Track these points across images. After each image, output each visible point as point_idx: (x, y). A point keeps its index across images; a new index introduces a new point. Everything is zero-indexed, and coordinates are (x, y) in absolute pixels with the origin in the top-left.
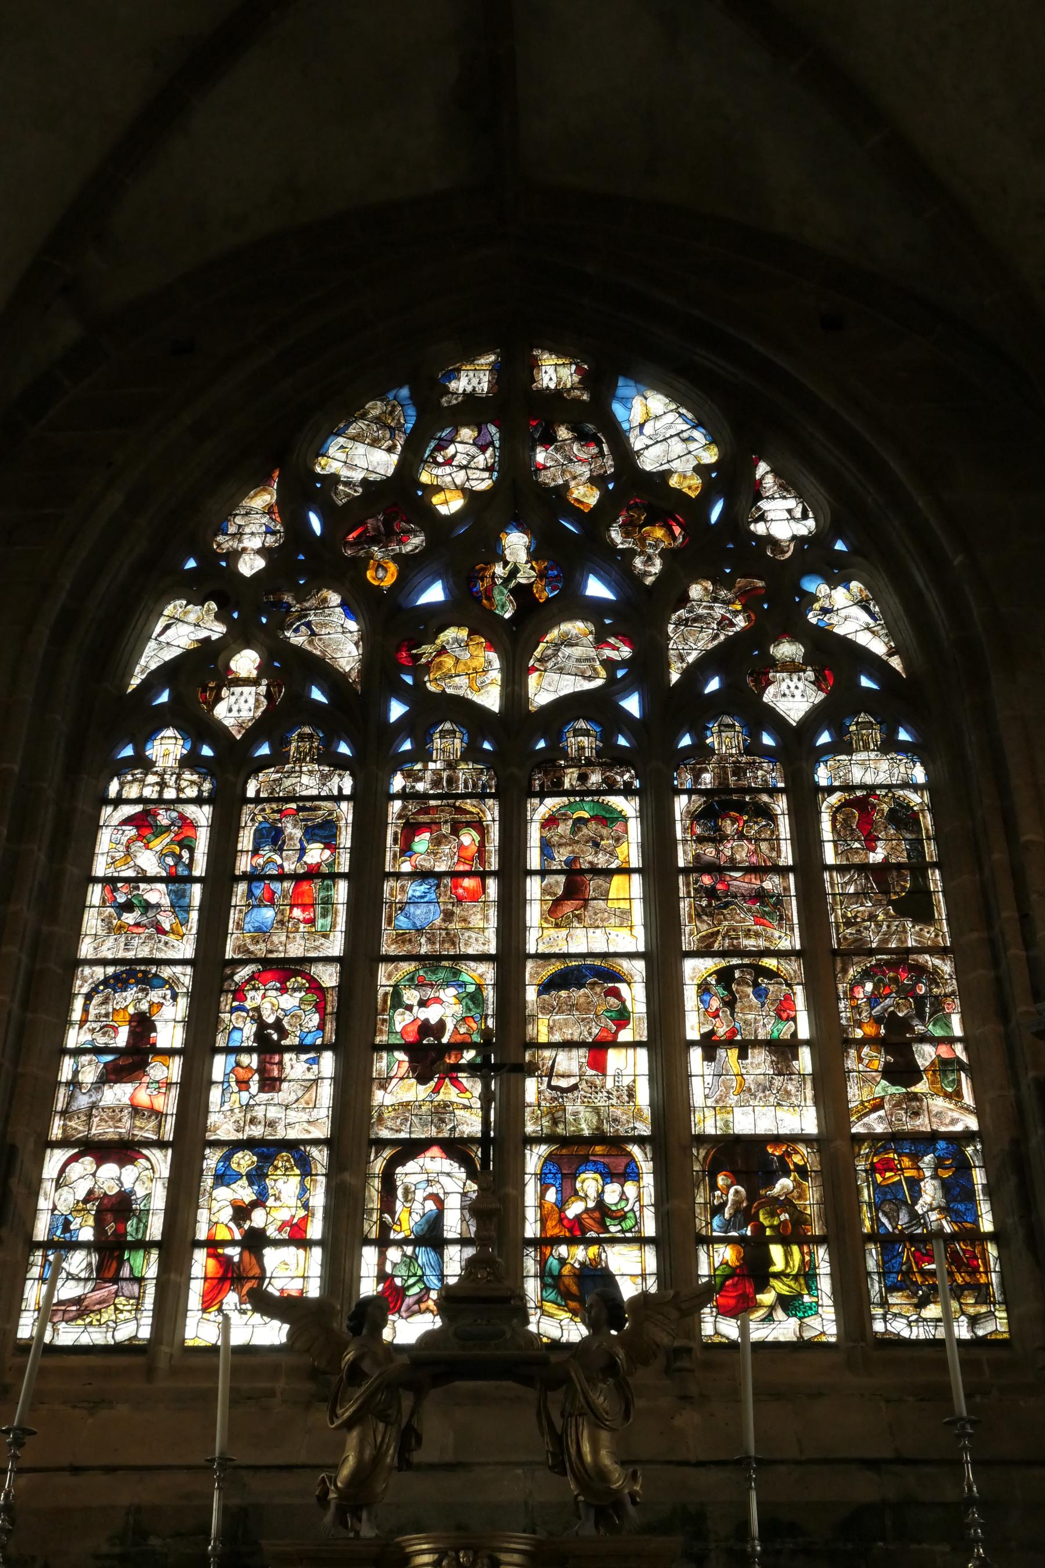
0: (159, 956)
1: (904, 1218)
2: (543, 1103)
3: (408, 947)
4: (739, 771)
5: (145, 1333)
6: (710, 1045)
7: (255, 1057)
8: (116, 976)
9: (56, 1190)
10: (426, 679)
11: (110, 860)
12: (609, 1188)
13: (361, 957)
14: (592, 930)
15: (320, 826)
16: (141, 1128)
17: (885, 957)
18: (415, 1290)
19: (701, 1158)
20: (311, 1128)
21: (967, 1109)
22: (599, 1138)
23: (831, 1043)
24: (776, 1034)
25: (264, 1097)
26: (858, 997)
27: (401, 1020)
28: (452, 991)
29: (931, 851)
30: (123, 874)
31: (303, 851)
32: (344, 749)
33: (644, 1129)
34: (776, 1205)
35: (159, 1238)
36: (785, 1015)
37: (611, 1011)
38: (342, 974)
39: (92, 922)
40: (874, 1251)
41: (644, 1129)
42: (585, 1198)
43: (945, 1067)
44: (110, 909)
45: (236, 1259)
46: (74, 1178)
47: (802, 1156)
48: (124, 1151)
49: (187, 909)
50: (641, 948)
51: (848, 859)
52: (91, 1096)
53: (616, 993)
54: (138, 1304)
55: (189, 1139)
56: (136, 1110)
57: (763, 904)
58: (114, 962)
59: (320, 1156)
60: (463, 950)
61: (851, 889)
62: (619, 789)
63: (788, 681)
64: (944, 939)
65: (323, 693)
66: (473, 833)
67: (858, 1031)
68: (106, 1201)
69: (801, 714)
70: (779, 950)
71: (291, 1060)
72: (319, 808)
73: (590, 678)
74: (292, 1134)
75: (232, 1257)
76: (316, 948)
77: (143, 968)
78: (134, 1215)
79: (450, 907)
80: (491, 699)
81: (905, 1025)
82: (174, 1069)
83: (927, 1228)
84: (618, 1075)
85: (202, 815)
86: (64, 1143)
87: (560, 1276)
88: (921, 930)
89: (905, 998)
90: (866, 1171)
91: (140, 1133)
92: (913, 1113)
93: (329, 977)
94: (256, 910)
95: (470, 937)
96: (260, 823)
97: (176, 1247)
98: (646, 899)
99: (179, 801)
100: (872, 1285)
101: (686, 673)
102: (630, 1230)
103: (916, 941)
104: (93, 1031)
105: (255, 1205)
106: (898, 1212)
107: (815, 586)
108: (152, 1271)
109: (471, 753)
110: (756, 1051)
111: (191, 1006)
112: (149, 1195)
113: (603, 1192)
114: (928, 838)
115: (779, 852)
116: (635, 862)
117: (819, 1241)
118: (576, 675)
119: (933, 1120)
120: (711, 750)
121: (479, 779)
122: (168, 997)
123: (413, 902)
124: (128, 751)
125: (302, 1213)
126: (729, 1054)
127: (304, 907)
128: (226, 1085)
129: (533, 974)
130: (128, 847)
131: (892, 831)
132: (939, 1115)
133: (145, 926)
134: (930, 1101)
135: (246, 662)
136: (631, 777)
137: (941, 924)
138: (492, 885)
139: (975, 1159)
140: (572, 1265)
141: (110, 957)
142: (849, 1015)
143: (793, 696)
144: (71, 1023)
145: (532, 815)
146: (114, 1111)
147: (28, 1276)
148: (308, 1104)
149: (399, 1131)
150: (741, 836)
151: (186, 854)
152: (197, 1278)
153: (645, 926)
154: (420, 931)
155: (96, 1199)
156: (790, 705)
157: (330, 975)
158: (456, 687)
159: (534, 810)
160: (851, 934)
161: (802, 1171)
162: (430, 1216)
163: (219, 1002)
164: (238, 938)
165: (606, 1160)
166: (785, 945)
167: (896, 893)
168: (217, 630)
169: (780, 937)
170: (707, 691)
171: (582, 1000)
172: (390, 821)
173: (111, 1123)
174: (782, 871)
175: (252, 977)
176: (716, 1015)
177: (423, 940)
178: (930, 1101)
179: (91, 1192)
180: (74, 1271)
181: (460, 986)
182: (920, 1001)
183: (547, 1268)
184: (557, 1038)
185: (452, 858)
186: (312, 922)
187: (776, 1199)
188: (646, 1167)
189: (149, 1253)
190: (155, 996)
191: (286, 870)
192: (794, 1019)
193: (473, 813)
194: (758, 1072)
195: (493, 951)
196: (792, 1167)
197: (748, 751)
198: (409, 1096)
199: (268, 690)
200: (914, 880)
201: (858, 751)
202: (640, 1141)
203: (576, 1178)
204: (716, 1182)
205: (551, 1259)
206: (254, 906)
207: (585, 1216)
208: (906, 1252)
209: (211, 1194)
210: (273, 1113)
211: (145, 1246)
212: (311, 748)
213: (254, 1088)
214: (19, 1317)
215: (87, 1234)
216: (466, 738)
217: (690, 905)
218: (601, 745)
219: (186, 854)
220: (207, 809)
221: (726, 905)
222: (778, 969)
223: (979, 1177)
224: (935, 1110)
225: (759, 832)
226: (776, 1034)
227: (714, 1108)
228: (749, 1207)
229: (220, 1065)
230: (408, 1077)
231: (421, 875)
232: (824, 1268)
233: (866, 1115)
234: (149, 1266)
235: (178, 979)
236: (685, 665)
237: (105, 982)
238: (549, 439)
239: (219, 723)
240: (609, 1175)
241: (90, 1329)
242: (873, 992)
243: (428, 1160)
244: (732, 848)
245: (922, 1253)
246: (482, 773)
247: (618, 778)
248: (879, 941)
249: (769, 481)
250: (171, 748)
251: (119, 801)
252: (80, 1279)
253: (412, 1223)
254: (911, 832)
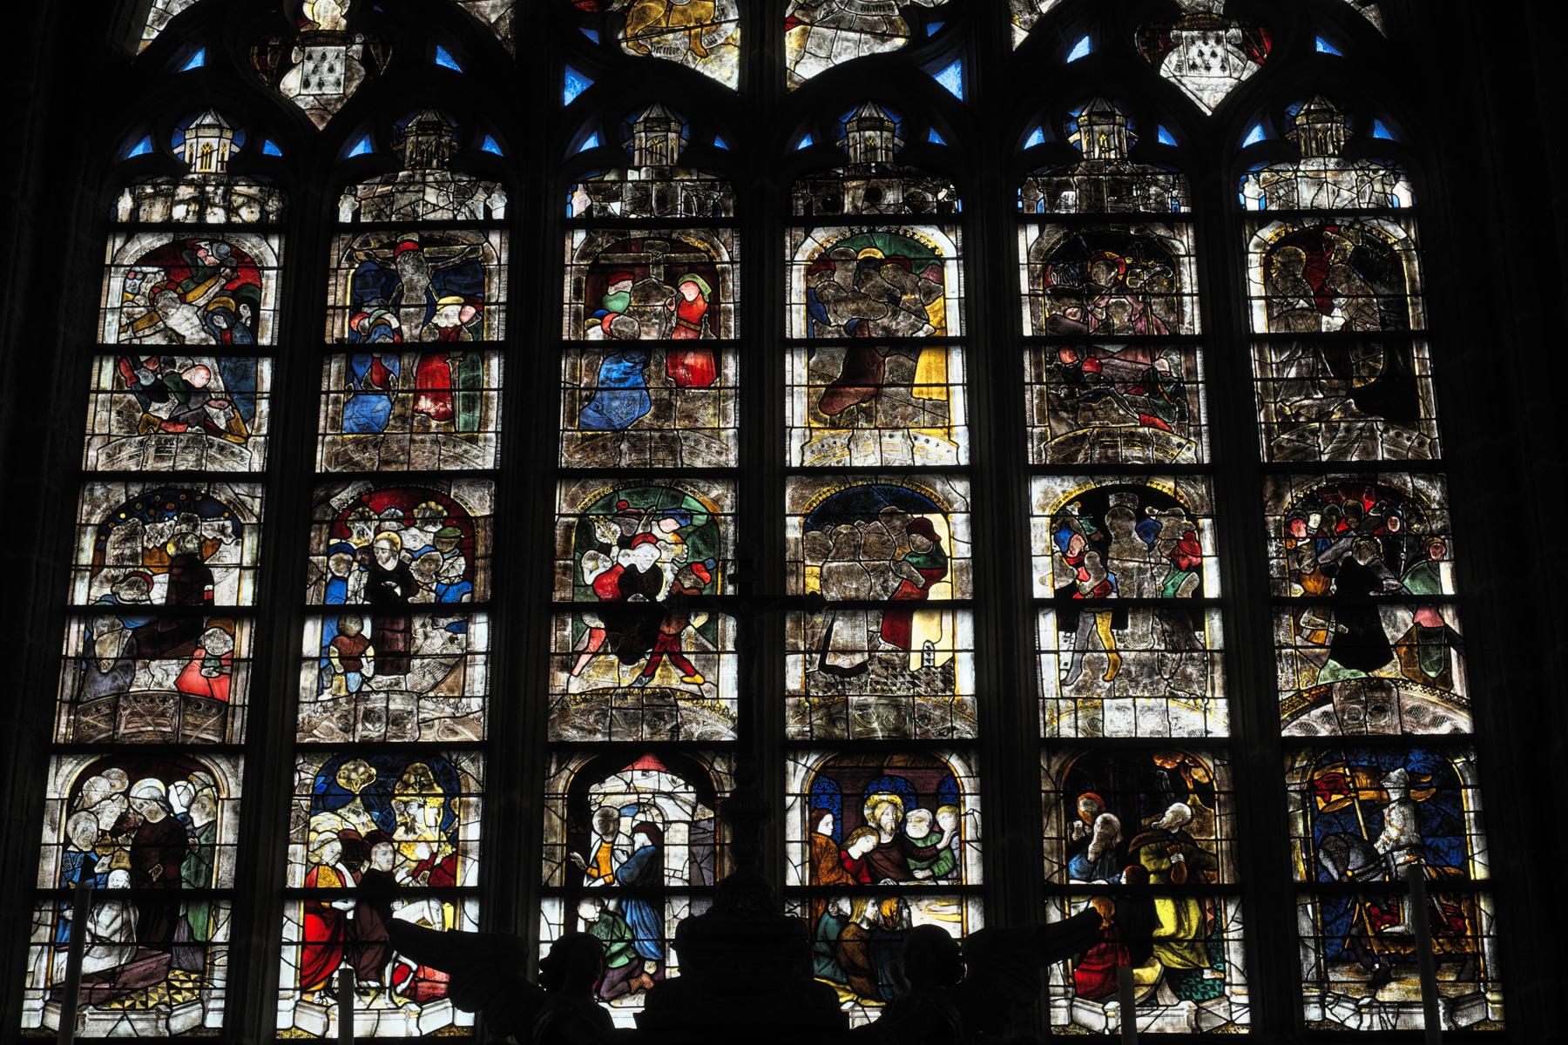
0: (211, 468)
1: (1356, 860)
2: (813, 692)
3: (601, 457)
4: (1120, 187)
5: (214, 1021)
7: (368, 624)
8: (143, 498)
9: (68, 818)
10: (620, 36)
11: (124, 321)
12: (914, 815)
13: (527, 472)
14: (888, 433)
15: (457, 269)
16: (196, 727)
17: (1340, 475)
18: (622, 961)
19: (1053, 772)
20: (459, 728)
21: (1458, 704)
22: (898, 743)
23: (1253, 604)
24: (1170, 591)
25: (384, 680)
26: (1297, 532)
27: (592, 569)
28: (670, 524)
29: (1415, 316)
30: (148, 341)
31: (432, 309)
32: (491, 147)
33: (965, 729)
34: (1166, 841)
35: (231, 885)
36: (1185, 562)
37: (918, 556)
38: (498, 500)
39: (101, 417)
40: (1309, 907)
41: (965, 729)
42: (878, 829)
43: (1425, 641)
44: (132, 397)
45: (350, 916)
46: (96, 797)
48: (171, 760)
49: (252, 397)
50: (964, 460)
51: (1288, 326)
52: (115, 679)
53: (927, 529)
54: (203, 980)
56: (185, 698)
57: (1155, 393)
58: (139, 477)
59: (472, 769)
60: (686, 461)
61: (1293, 373)
62: (931, 213)
63: (1200, 43)
64: (1432, 448)
65: (455, 59)
66: (700, 281)
67: (1297, 586)
68: (146, 832)
69: (1220, 96)
70: (1178, 465)
71: (423, 625)
72: (453, 241)
73: (883, 38)
74: (429, 736)
75: (344, 912)
76: (457, 458)
77: (186, 486)
78: (192, 852)
79: (665, 394)
80: (725, 70)
81: (1369, 577)
83: (1390, 874)
84: (929, 650)
85: (269, 251)
86: (74, 749)
87: (839, 940)
88: (1398, 435)
89: (1370, 538)
90: (1301, 792)
91: (195, 734)
92: (1376, 708)
93: (479, 504)
94: (361, 397)
95: (697, 442)
96: (362, 263)
98: (971, 387)
99: (229, 227)
100: (1306, 956)
101: (1035, 30)
102: (944, 877)
103: (1389, 451)
104: (113, 581)
105: (375, 838)
106: (1348, 850)
108: (221, 936)
110: (1140, 617)
111: (262, 545)
112: (212, 825)
113: (905, 821)
114: (1414, 294)
115: (1181, 314)
116: (954, 329)
117: (1227, 893)
118: (861, 31)
119: (1406, 718)
120: (1075, 153)
121: (709, 197)
122: (230, 530)
123: (611, 387)
125: (449, 850)
126: (1099, 620)
127: (437, 396)
128: (325, 662)
130: (152, 300)
131: (1358, 283)
132: (1416, 711)
133: (187, 423)
134: (1402, 692)
136: (948, 196)
137: (1430, 428)
138: (731, 368)
139: (1467, 775)
140: (858, 926)
141: (134, 468)
142: (1282, 562)
143: (1208, 68)
144: (79, 569)
145: (793, 255)
146: (152, 701)
147: (33, 940)
148: (452, 691)
149: (594, 732)
150: (1122, 289)
151: (245, 312)
152: (291, 943)
153: (970, 425)
154: (620, 433)
155: (133, 829)
156: (1204, 81)
157: (481, 499)
158: (670, 50)
159: (796, 247)
160: (1289, 440)
161: (1205, 791)
162: (642, 856)
163: (309, 539)
164: (334, 442)
165: (910, 774)
166: (1186, 456)
167: (1360, 379)
169: (1180, 446)
170: (1071, 59)
171: (873, 538)
172: (567, 261)
173: (149, 719)
174: (1185, 345)
175: (358, 502)
176: (1078, 562)
177: (624, 447)
178: (1402, 692)
179: (122, 819)
180: (101, 932)
181: (683, 516)
182: (1392, 543)
183: (820, 930)
184: (833, 594)
185: (668, 320)
186: (449, 417)
187: (1165, 832)
188: (968, 785)
189: (218, 908)
190: (208, 530)
191: (406, 336)
192: (1199, 569)
193: (699, 250)
194: (1143, 646)
195: (733, 464)
196: (1190, 786)
197: (1135, 154)
198: (605, 681)
199: (366, 52)
200: (1391, 362)
201: (1309, 156)
202: (961, 748)
203: (864, 802)
204: (1076, 808)
205: (826, 917)
206: (356, 393)
207: (877, 856)
208: (1359, 910)
209: (308, 824)
210: (397, 704)
211: (210, 898)
212: (439, 144)
213: (368, 669)
214: (22, 998)
215: (119, 879)
216: (685, 133)
217: (1041, 393)
218: (902, 144)
219: (245, 312)
220: (275, 243)
221: (1097, 396)
222: (1176, 492)
223: (1469, 802)
224: (1409, 704)
225: (1150, 283)
226: (1170, 591)
227: (1075, 700)
228: (1125, 842)
229: (312, 637)
230: (605, 653)
231: (616, 346)
232: (1234, 932)
233: (1306, 710)
235: (243, 503)
236: (1036, 17)
237: (129, 507)
239: (289, 103)
240: (913, 799)
241: (133, 1017)
242: (1320, 528)
243: (638, 774)
244: (1107, 307)
245: (1382, 911)
246: (713, 187)
247: (930, 197)
248: (1333, 451)
250: (214, 143)
251: (134, 228)
252: (114, 944)
253: (616, 866)
254: (1390, 285)
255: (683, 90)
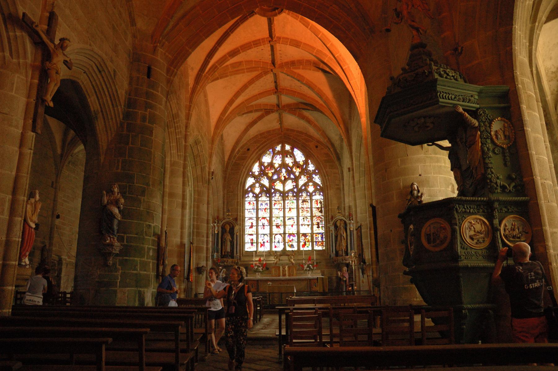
6: (302, 225)
23: (312, 225)
47: (309, 235)
48: (252, 235)
55: (257, 234)
82: (255, 227)
85: (255, 202)
97: (257, 243)
107: (314, 176)
109: (280, 196)
124: (247, 196)
129: (287, 218)
135: (257, 185)
168: (254, 181)
234: (255, 244)
238: (287, 157)
249: (310, 163)
255: (279, 191)
